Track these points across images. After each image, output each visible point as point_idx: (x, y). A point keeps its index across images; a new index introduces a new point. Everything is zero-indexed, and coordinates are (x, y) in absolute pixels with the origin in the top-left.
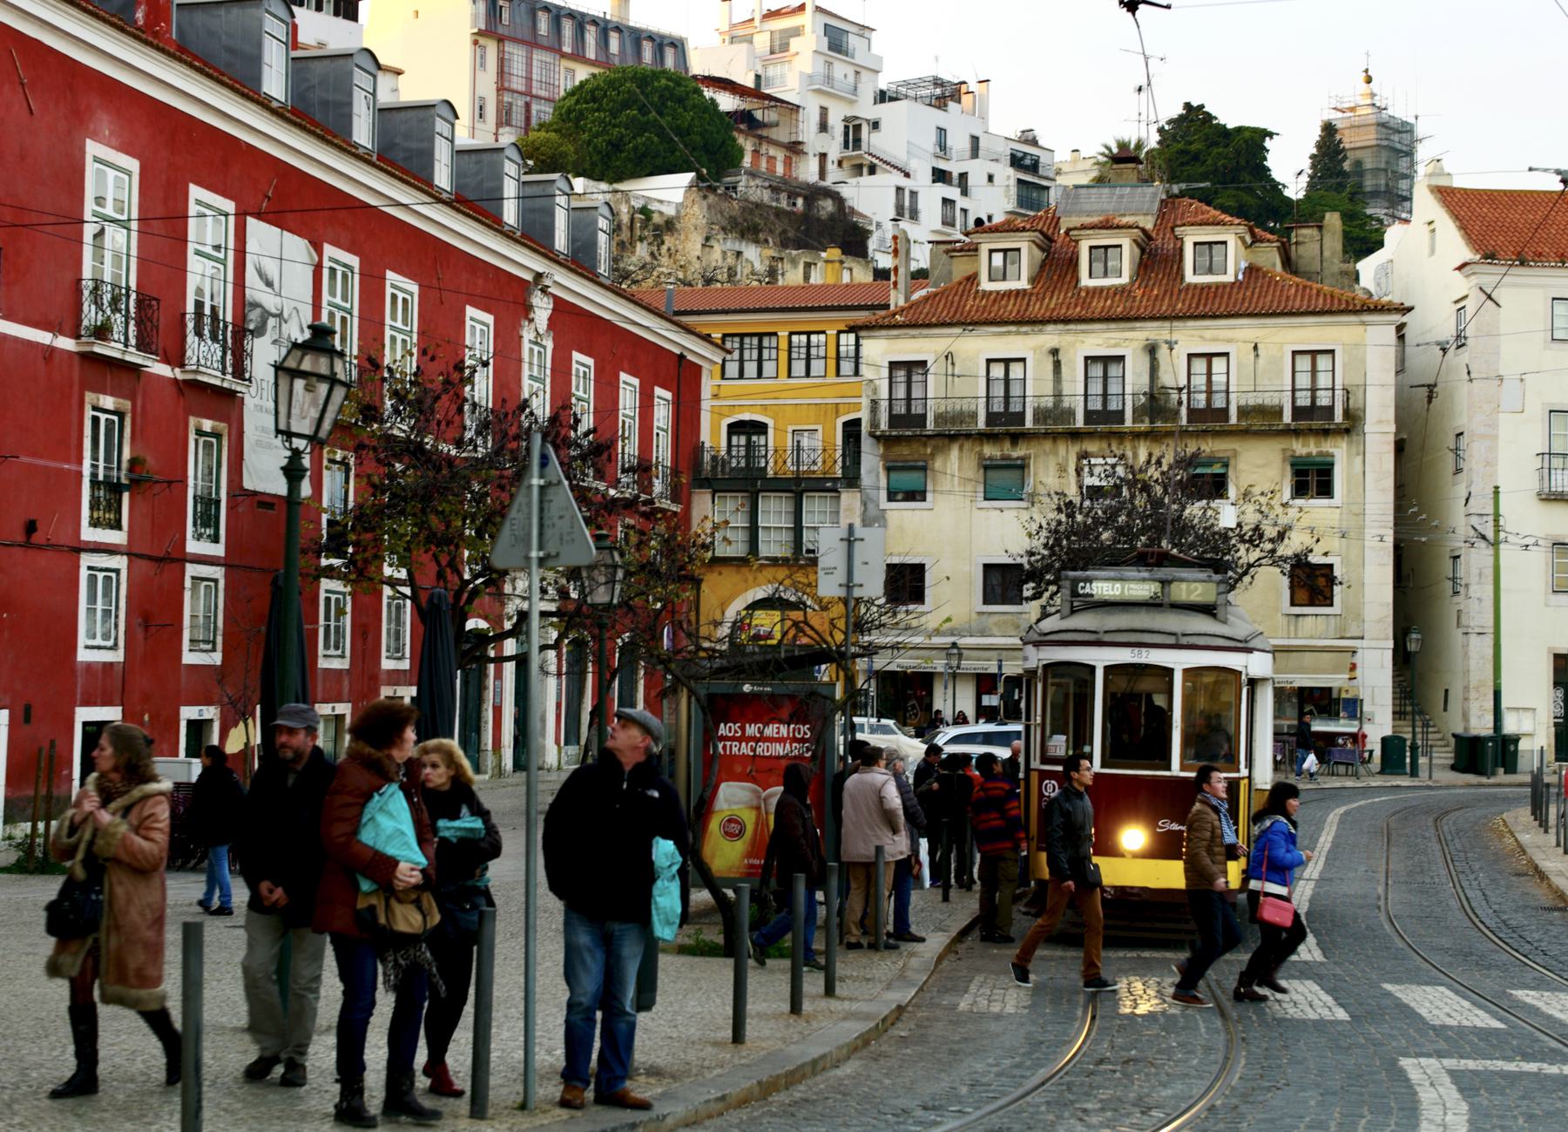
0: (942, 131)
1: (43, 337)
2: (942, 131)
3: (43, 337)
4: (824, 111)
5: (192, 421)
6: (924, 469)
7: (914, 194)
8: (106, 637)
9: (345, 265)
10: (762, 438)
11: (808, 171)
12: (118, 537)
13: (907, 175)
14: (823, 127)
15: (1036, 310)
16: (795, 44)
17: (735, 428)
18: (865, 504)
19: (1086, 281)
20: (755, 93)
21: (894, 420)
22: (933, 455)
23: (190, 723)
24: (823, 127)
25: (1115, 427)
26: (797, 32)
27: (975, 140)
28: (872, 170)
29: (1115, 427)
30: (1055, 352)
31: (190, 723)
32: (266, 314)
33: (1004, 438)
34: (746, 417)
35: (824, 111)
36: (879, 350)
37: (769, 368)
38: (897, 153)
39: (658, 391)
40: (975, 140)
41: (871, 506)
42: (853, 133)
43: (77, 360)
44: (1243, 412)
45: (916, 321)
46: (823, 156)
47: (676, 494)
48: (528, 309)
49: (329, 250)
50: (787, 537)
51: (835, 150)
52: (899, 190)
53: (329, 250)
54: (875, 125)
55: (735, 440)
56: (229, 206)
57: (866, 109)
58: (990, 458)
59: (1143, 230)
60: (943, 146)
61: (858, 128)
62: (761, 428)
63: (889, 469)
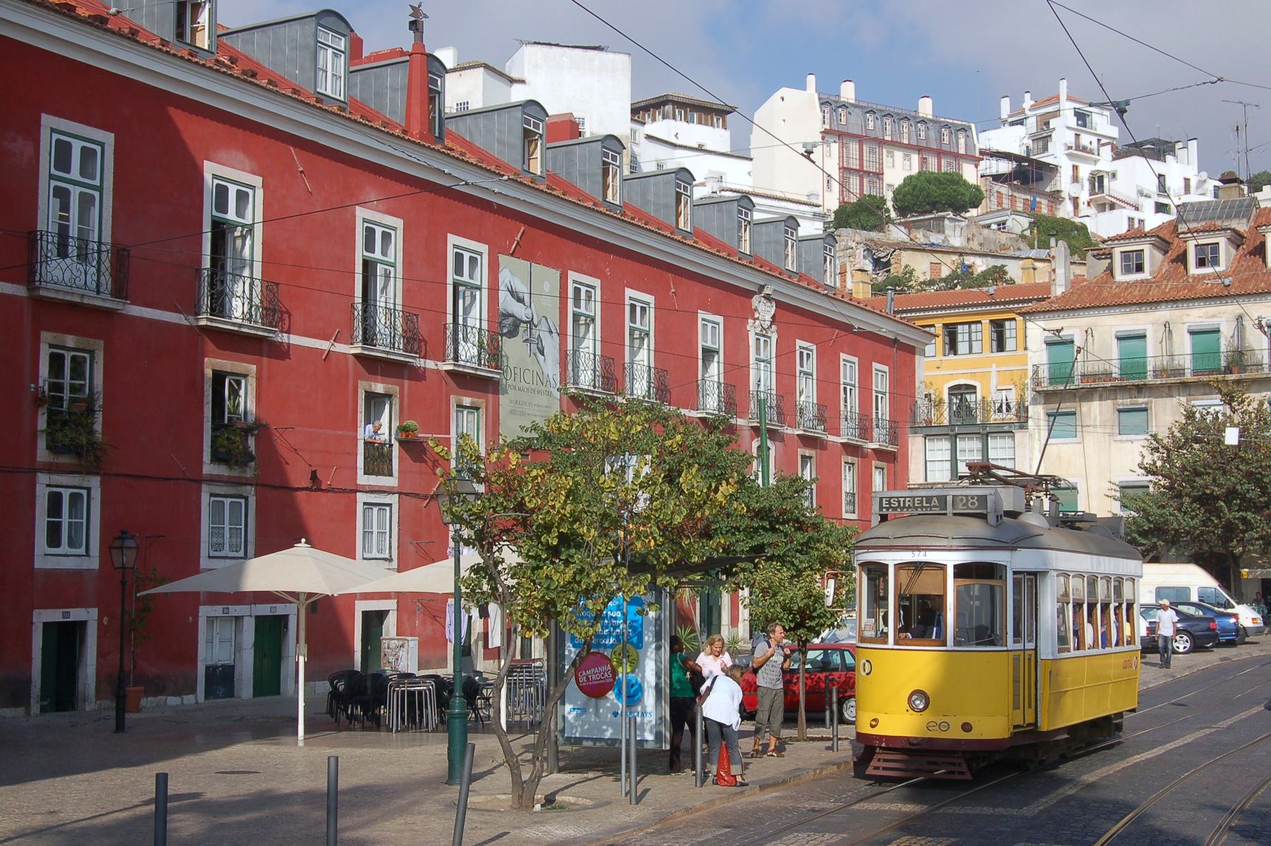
0: (1161, 177)
1: (324, 345)
2: (1161, 177)
3: (324, 345)
4: (1075, 168)
5: (453, 399)
6: (1074, 414)
7: (1141, 221)
8: (380, 550)
9: (588, 286)
11: (1065, 211)
12: (391, 482)
13: (1137, 209)
14: (1075, 179)
15: (1154, 294)
16: (1053, 123)
19: (1193, 270)
20: (1027, 159)
21: (1053, 380)
23: (365, 614)
24: (1075, 179)
26: (1056, 114)
27: (1187, 180)
28: (1112, 207)
30: (1166, 324)
31: (365, 614)
32: (517, 322)
33: (1131, 386)
34: (962, 382)
35: (1075, 168)
36: (1037, 331)
37: (976, 346)
38: (1132, 196)
39: (875, 365)
40: (1187, 180)
42: (1097, 181)
43: (352, 359)
45: (1067, 308)
46: (1075, 201)
47: (894, 436)
48: (752, 312)
49: (572, 276)
51: (1084, 196)
52: (1131, 220)
53: (572, 276)
54: (1114, 175)
56: (484, 248)
57: (1105, 162)
59: (1234, 230)
60: (1162, 188)
61: (1101, 179)
62: (971, 389)
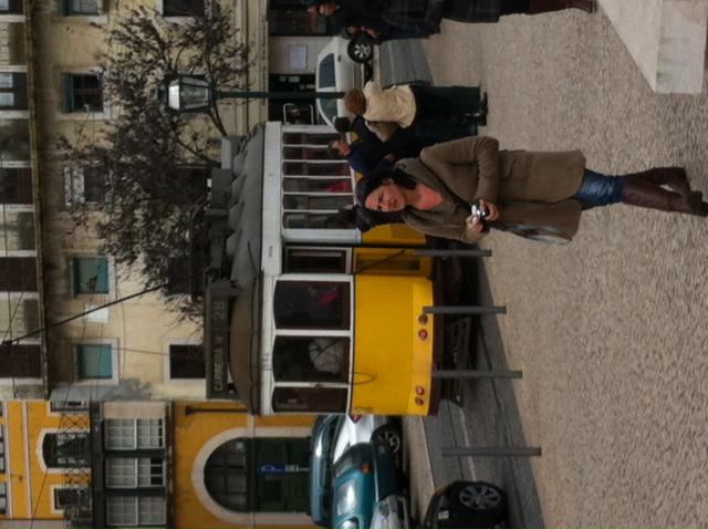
10: (59, 437)
17: (50, 461)
18: (114, 398)
22: (66, 339)
25: (35, 180)
29: (35, 180)
34: (39, 452)
41: (116, 393)
44: (16, 59)
50: (148, 502)
55: (60, 461)
58: (68, 288)
62: (50, 441)
63: (82, 376)
